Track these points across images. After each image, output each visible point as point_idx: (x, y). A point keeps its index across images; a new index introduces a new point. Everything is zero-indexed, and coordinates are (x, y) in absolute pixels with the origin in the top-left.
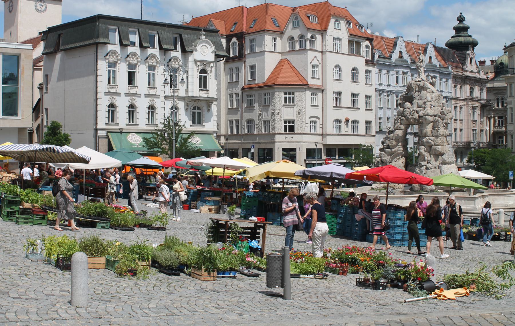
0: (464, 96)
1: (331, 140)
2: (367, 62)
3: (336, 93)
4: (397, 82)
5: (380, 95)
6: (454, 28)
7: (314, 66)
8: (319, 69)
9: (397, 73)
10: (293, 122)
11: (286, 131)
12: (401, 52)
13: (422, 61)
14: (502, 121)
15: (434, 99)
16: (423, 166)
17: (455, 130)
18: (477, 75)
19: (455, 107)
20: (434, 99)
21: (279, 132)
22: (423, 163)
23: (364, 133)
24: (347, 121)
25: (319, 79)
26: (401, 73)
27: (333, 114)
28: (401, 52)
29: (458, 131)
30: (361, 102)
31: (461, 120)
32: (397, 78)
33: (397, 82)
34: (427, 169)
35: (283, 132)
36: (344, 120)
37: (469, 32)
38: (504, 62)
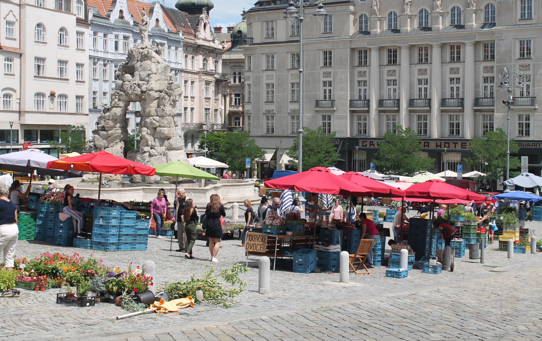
0: (196, 69)
1: (31, 120)
3: (38, 59)
4: (116, 48)
5: (95, 64)
7: (9, 23)
8: (16, 27)
9: (117, 37)
12: (121, 11)
13: (146, 24)
14: (239, 99)
15: (160, 71)
16: (146, 152)
17: (186, 109)
18: (211, 44)
19: (186, 82)
20: (160, 71)
22: (146, 149)
23: (74, 111)
24: (52, 95)
25: (15, 40)
26: (121, 37)
27: (33, 85)
28: (121, 11)
29: (189, 110)
30: (71, 71)
31: (193, 98)
32: (116, 43)
33: (116, 48)
34: (150, 155)
36: (48, 94)
38: (242, 30)
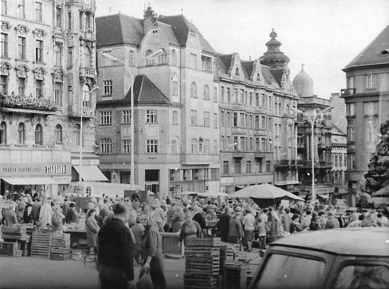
6: (267, 45)
11: (148, 151)
36: (198, 139)
37: (281, 49)
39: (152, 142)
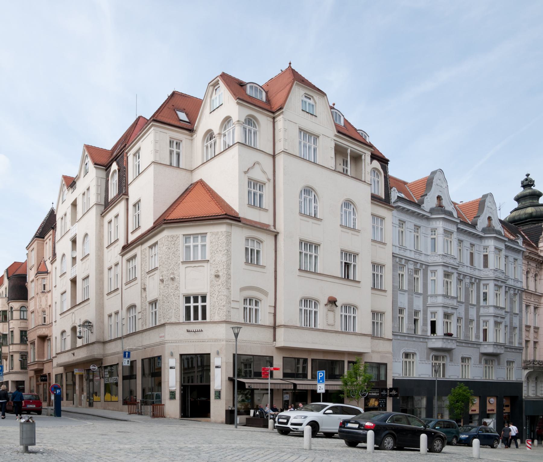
2: (375, 198)
10: (204, 299)
11: (188, 317)
17: (527, 342)
19: (527, 306)
21: (173, 320)
25: (266, 210)
29: (531, 344)
35: (182, 318)
39: (196, 300)
